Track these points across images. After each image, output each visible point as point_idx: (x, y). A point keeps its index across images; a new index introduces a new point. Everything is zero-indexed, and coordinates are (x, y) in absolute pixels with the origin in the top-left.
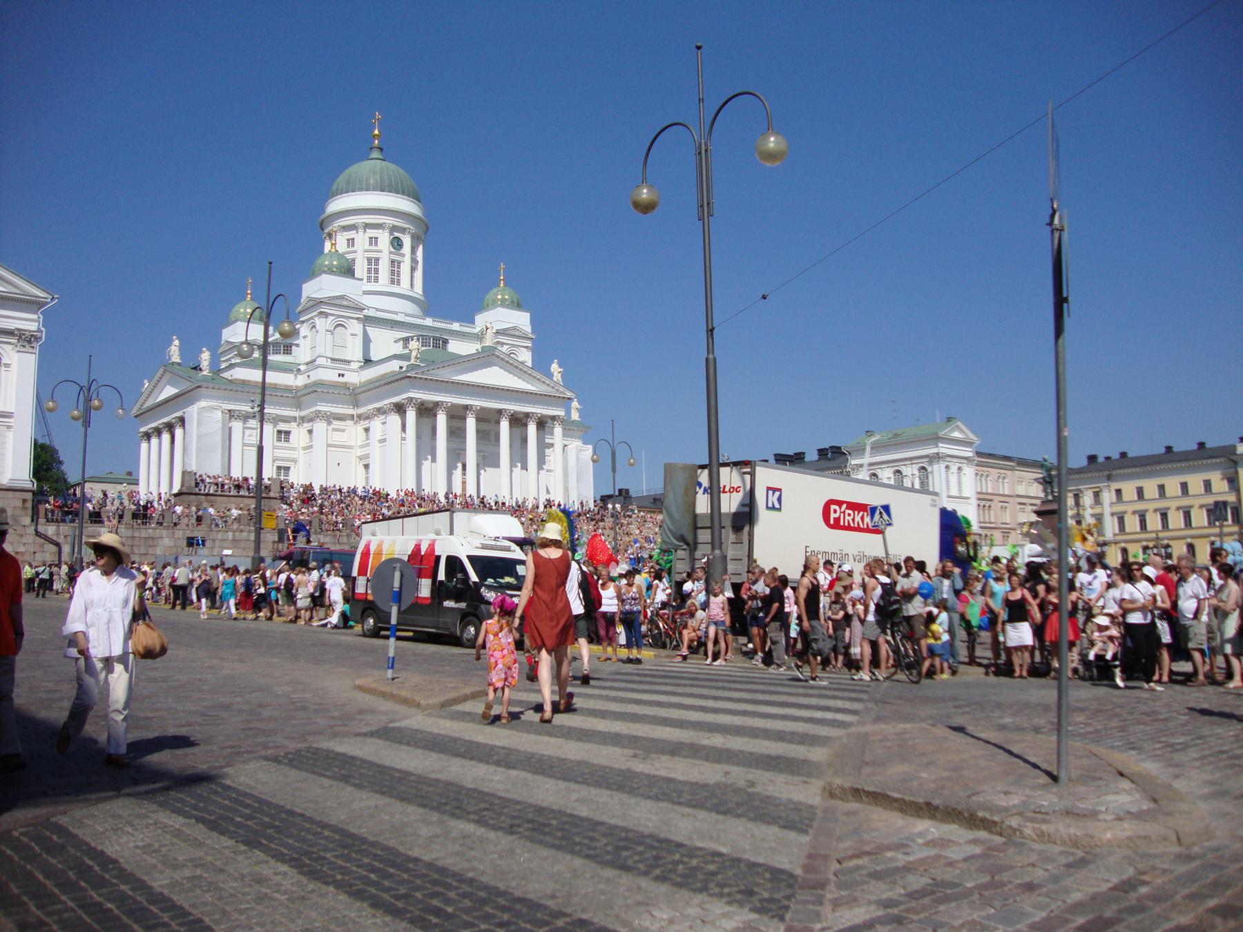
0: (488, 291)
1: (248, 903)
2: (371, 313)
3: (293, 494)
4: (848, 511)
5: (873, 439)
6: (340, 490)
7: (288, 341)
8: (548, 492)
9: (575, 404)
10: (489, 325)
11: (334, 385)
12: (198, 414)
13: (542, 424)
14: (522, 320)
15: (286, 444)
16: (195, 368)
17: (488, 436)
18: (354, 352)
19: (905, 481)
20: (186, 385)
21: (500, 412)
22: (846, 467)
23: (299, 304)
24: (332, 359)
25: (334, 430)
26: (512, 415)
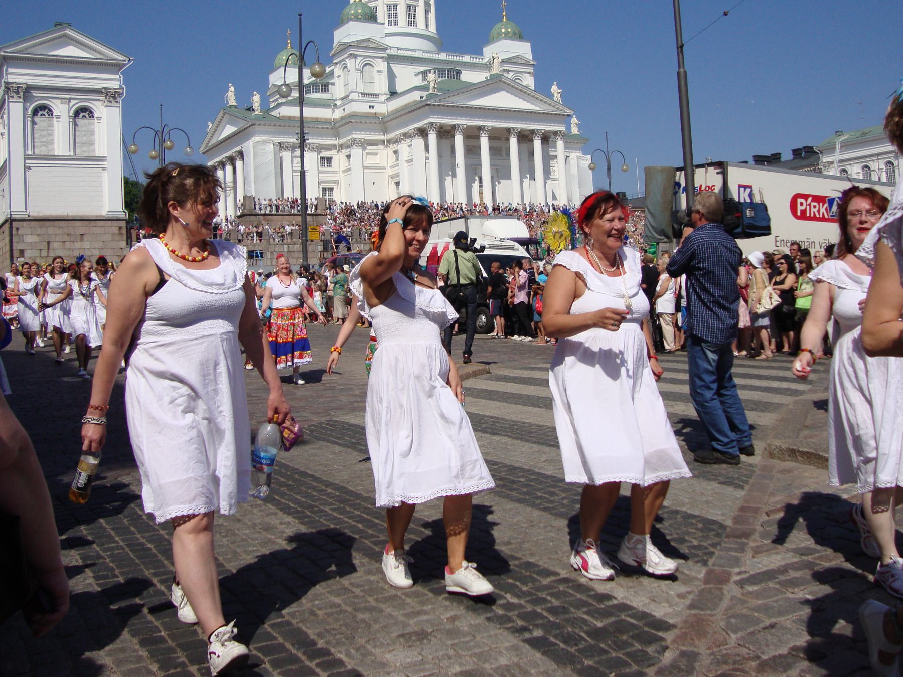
0: (492, 27)
1: (255, 546)
2: (393, 52)
3: (337, 209)
4: (813, 204)
5: (842, 138)
6: (377, 205)
7: (325, 81)
8: (554, 198)
9: (574, 120)
10: (495, 56)
11: (366, 116)
12: (254, 148)
13: (546, 139)
14: (524, 49)
15: (329, 169)
16: (249, 109)
17: (499, 152)
18: (381, 86)
19: (873, 175)
20: (243, 124)
21: (509, 131)
22: (818, 165)
23: (332, 48)
24: (363, 94)
25: (368, 154)
26: (520, 132)
